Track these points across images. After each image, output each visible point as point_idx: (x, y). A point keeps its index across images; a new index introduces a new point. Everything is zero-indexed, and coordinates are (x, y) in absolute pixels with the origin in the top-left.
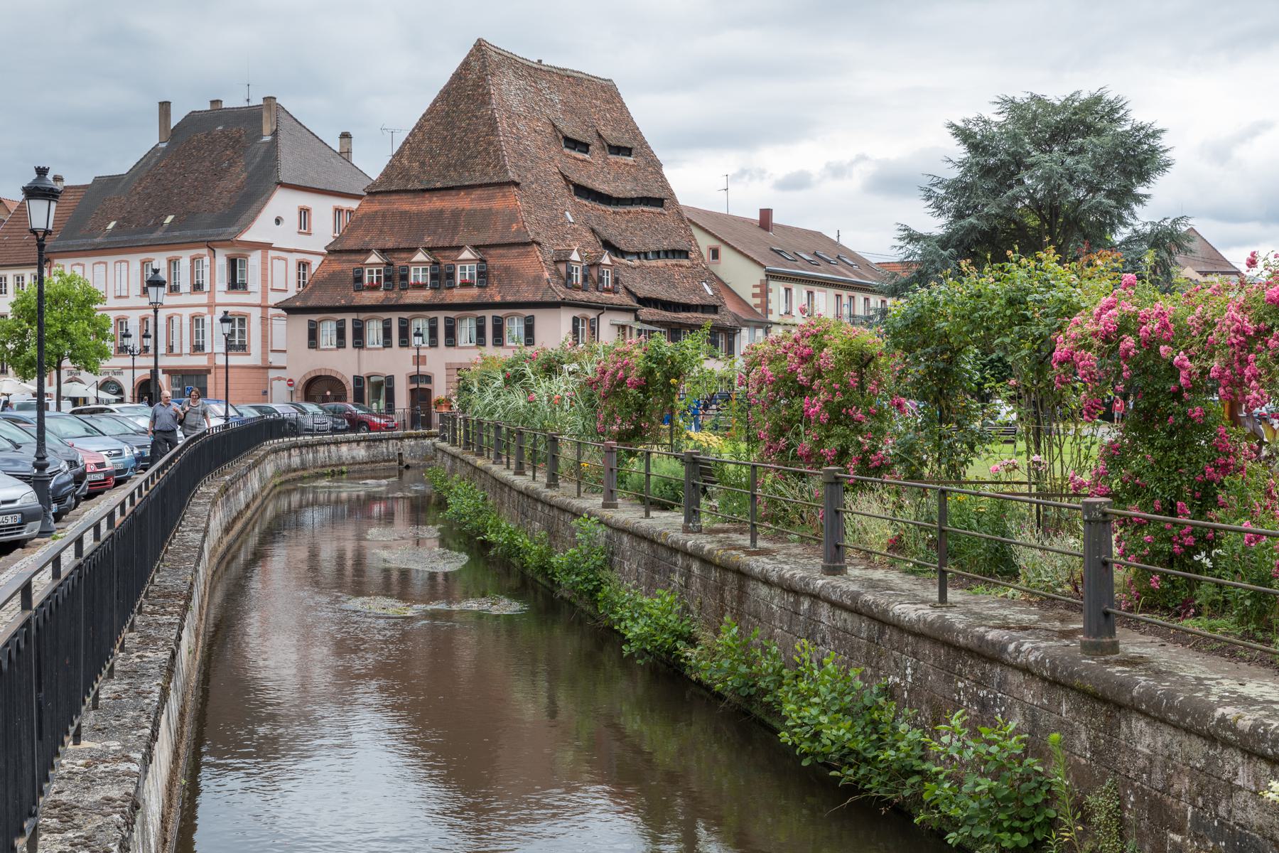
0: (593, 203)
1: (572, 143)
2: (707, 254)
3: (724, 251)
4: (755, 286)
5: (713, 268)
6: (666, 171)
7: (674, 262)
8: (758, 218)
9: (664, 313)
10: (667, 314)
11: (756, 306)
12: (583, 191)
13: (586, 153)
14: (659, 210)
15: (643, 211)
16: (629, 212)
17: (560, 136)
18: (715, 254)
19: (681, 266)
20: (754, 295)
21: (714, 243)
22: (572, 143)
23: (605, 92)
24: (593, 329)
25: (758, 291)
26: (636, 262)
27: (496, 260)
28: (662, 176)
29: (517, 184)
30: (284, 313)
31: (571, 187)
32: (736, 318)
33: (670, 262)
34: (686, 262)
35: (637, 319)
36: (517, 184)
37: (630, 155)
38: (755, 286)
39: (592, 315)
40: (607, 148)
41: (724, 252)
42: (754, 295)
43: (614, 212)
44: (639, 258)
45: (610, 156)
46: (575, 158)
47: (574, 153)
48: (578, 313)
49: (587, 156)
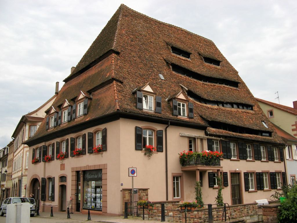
0: (187, 77)
1: (176, 50)
2: (267, 114)
3: (275, 111)
4: (293, 125)
5: (271, 120)
6: (239, 74)
7: (243, 110)
8: (292, 106)
9: (230, 132)
10: (234, 133)
11: (295, 135)
12: (177, 68)
13: (189, 58)
14: (235, 88)
15: (224, 87)
16: (214, 86)
17: (170, 47)
18: (271, 113)
19: (248, 113)
20: (293, 130)
21: (270, 108)
22: (176, 50)
23: (207, 42)
24: (162, 138)
25: (294, 127)
26: (216, 107)
27: (97, 95)
28: (238, 76)
29: (118, 53)
30: (26, 145)
31: (171, 67)
32: (283, 139)
33: (240, 110)
34: (251, 111)
35: (206, 134)
36: (118, 53)
37: (219, 65)
38: (293, 125)
39: (159, 127)
40: (203, 59)
41: (275, 111)
42: (293, 130)
43: (203, 84)
44: (218, 105)
45: (206, 63)
46: (179, 58)
47: (178, 56)
48: (141, 125)
49: (188, 59)
